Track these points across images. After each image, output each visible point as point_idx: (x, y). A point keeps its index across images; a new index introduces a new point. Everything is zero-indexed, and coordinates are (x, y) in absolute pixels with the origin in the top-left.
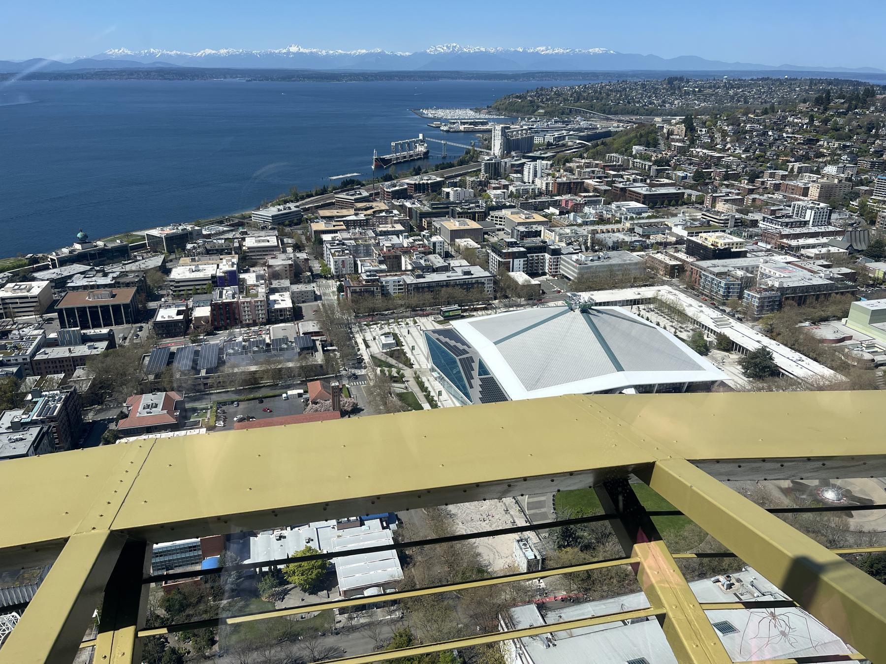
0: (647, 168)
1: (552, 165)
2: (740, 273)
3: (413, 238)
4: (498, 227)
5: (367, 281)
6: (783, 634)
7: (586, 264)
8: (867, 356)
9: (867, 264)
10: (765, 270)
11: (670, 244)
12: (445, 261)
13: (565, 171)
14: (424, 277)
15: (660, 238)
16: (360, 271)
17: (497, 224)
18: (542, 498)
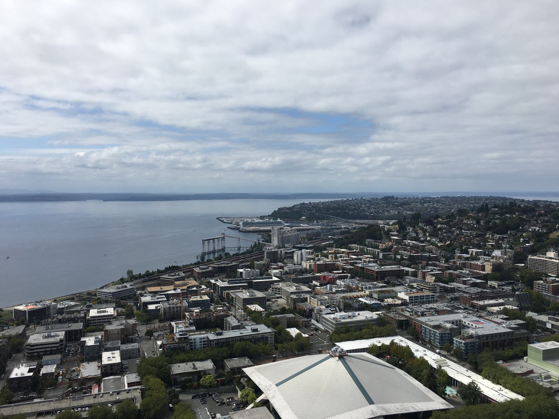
0: (376, 253)
2: (449, 325)
4: (277, 295)
5: (180, 339)
7: (340, 321)
8: (548, 385)
11: (398, 305)
12: (239, 322)
13: (322, 256)
15: (390, 301)
17: (276, 293)
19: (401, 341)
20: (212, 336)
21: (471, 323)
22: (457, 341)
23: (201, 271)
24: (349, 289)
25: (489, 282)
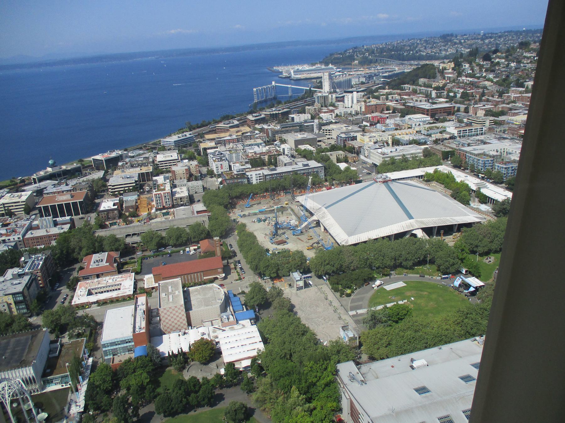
0: (429, 92)
1: (363, 96)
2: (492, 153)
3: (269, 146)
4: (328, 136)
11: (446, 139)
13: (373, 98)
15: (439, 136)
16: (233, 169)
18: (360, 303)
19: (445, 168)
20: (266, 172)
21: (514, 151)
22: (498, 166)
23: (253, 119)
24: (398, 127)
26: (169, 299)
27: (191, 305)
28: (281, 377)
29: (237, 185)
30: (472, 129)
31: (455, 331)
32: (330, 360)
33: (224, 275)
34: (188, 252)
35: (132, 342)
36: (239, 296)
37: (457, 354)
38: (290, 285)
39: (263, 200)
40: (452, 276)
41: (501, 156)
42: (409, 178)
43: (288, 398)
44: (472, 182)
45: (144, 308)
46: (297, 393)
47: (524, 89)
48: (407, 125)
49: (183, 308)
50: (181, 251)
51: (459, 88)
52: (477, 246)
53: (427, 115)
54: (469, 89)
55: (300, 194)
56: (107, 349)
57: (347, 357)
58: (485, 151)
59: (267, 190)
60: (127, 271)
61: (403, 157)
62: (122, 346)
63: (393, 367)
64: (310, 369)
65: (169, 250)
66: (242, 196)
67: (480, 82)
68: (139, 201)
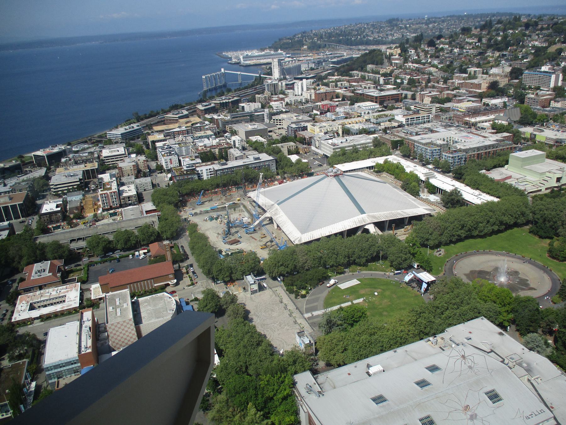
0: (377, 79)
1: (313, 83)
2: (440, 142)
6: (470, 367)
9: (520, 130)
10: (455, 138)
11: (395, 127)
14: (227, 165)
15: (388, 124)
17: (277, 124)
18: (315, 304)
19: (394, 158)
20: (216, 166)
22: (445, 156)
23: (203, 108)
24: (348, 116)
25: (483, 100)
26: (116, 313)
27: (141, 317)
28: (237, 393)
29: (188, 181)
30: (419, 117)
31: (409, 331)
32: (287, 371)
33: (175, 281)
34: (137, 256)
35: (78, 363)
36: (191, 304)
37: (412, 357)
38: (244, 288)
39: (214, 197)
40: (405, 271)
41: (447, 144)
42: (360, 169)
43: (244, 416)
44: (421, 172)
45: (90, 324)
46: (253, 411)
47: (467, 75)
48: (356, 114)
49: (132, 322)
50: (131, 256)
51: (406, 74)
52: (427, 240)
53: (376, 102)
54: (416, 75)
55: (253, 189)
56: (50, 372)
57: (304, 367)
58: (433, 140)
59: (218, 186)
60: (73, 281)
61: (353, 147)
62: (68, 367)
63: (349, 374)
64: (266, 383)
65: (117, 255)
66: (193, 193)
67: (425, 68)
68: (84, 201)
